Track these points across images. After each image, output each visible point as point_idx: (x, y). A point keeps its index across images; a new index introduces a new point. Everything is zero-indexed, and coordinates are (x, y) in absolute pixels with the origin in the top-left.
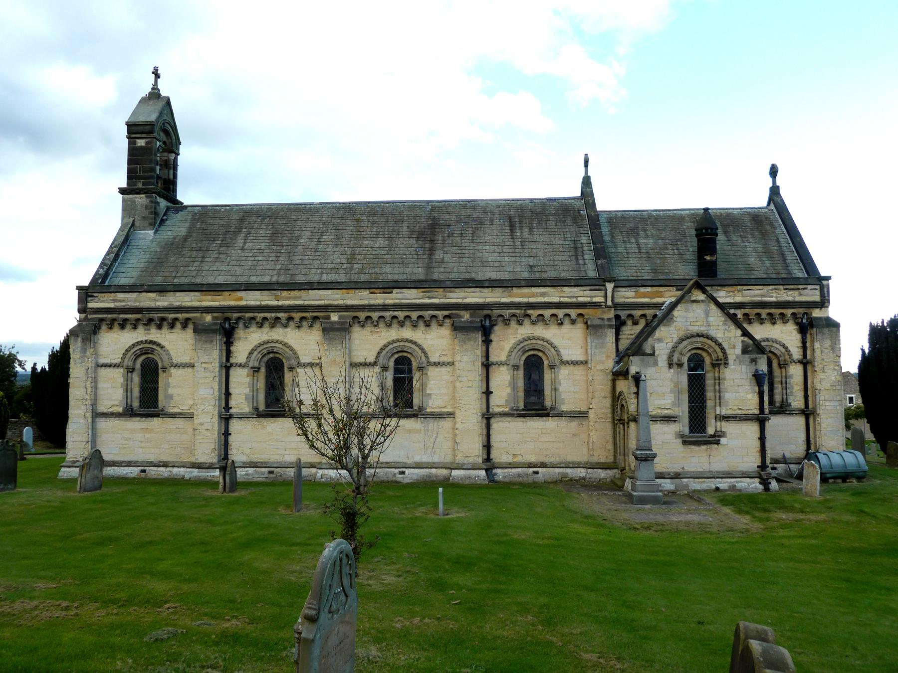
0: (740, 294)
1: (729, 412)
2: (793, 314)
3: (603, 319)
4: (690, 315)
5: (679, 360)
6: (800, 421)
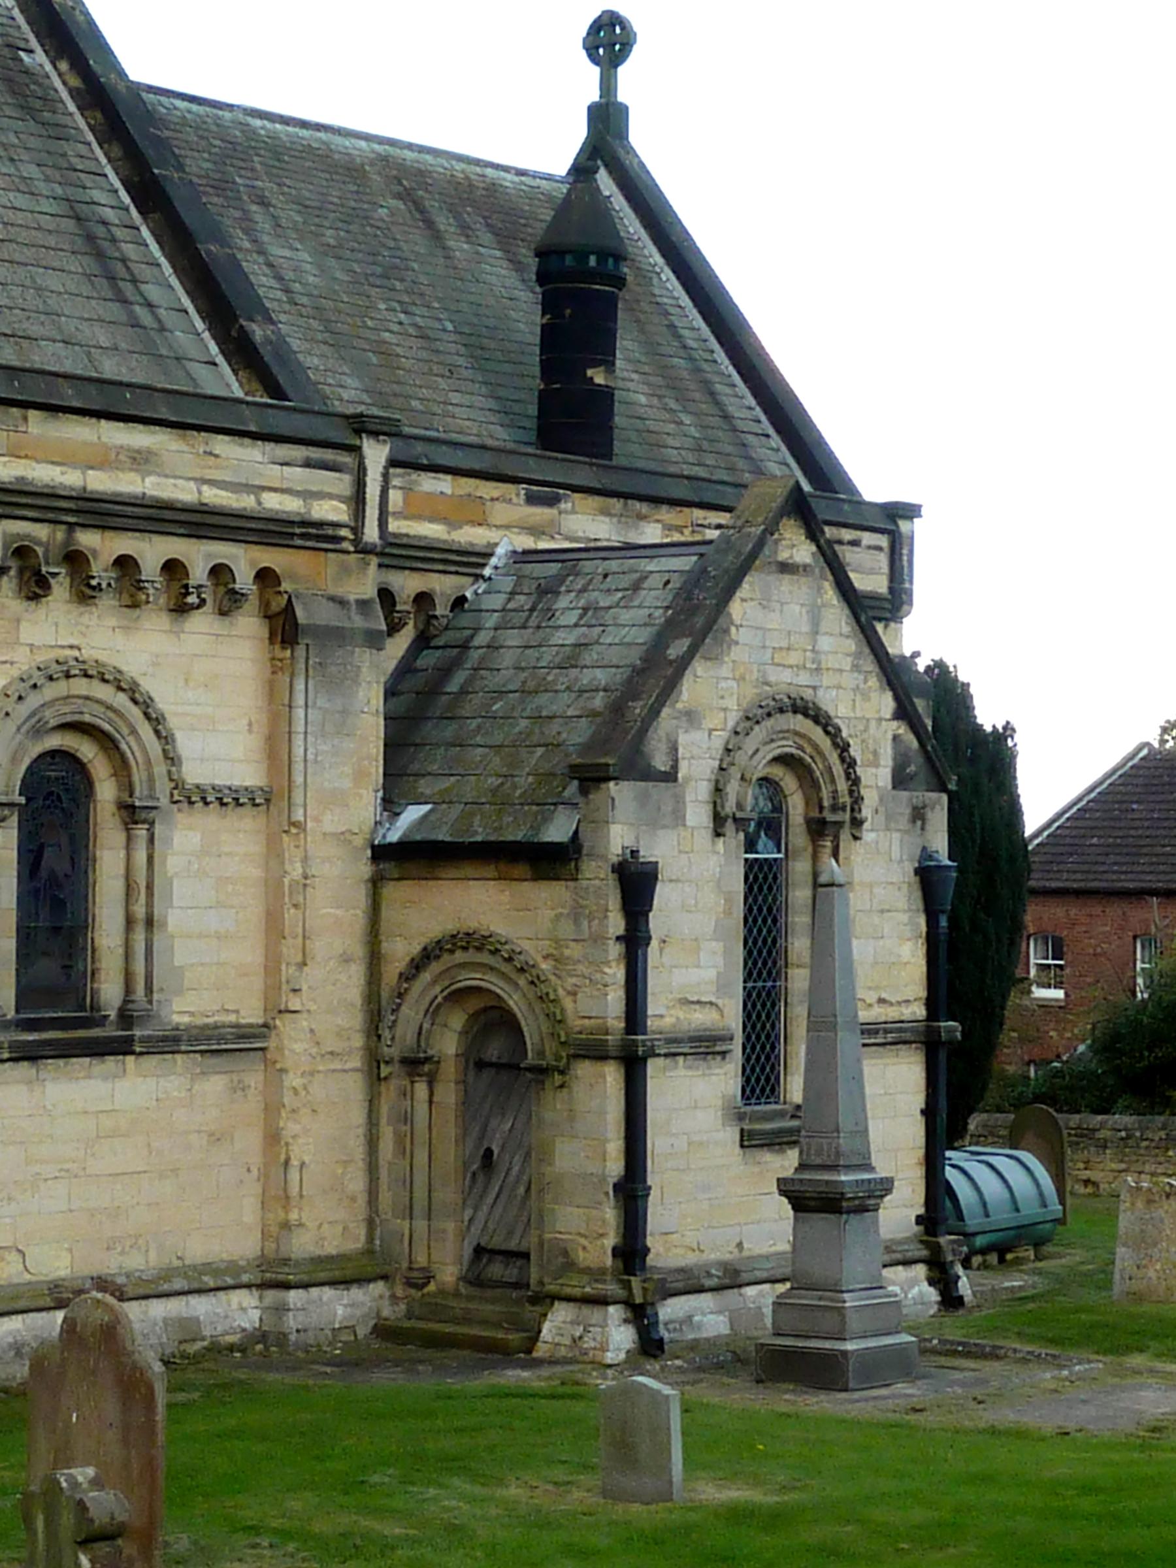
3: (342, 602)
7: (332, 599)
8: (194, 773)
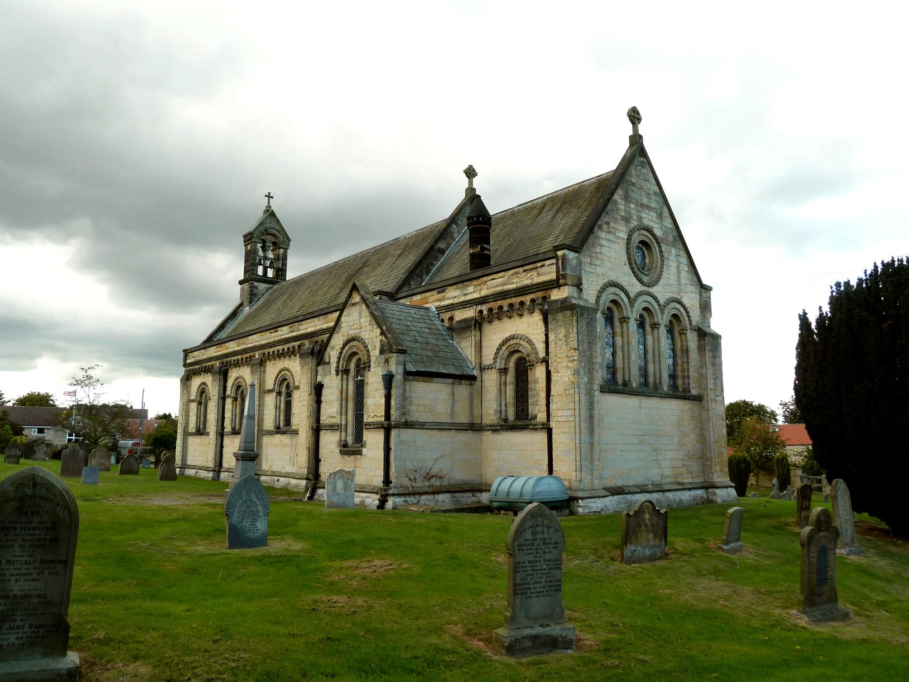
0: (485, 287)
6: (542, 437)
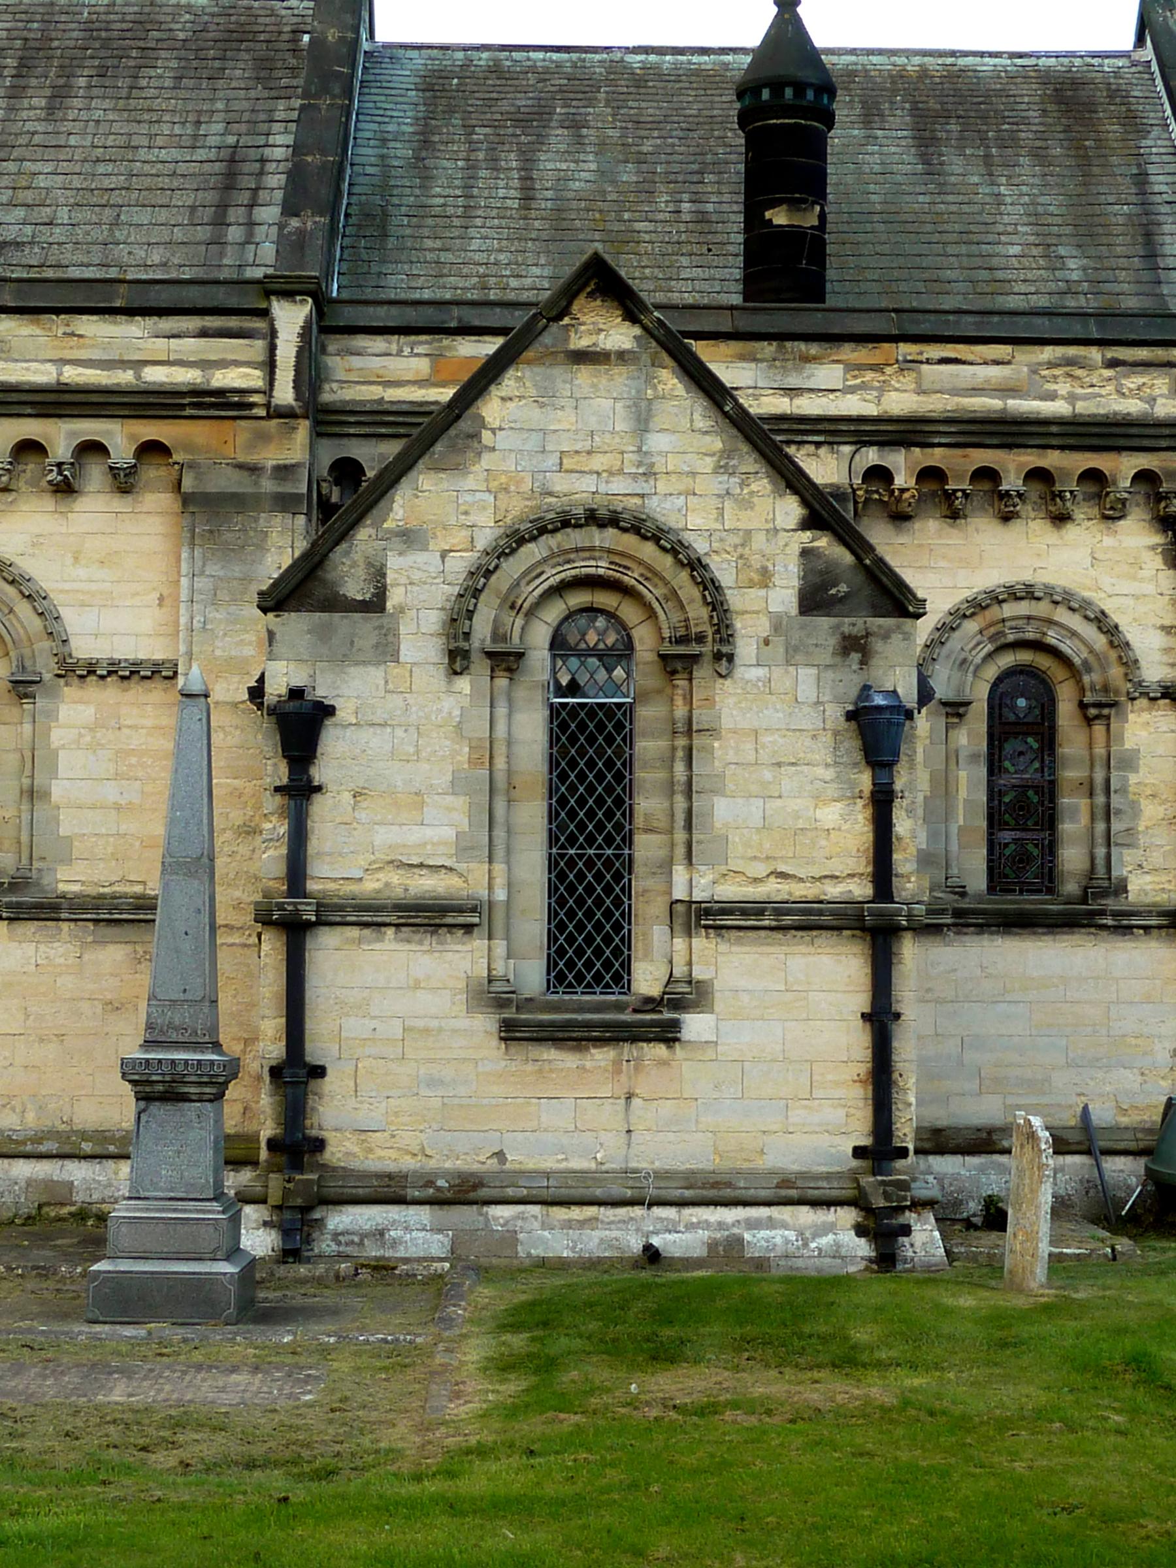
0: (908, 380)
1: (730, 891)
2: (1144, 477)
3: (253, 469)
4: (563, 419)
5: (498, 635)
7: (240, 466)
8: (83, 648)
